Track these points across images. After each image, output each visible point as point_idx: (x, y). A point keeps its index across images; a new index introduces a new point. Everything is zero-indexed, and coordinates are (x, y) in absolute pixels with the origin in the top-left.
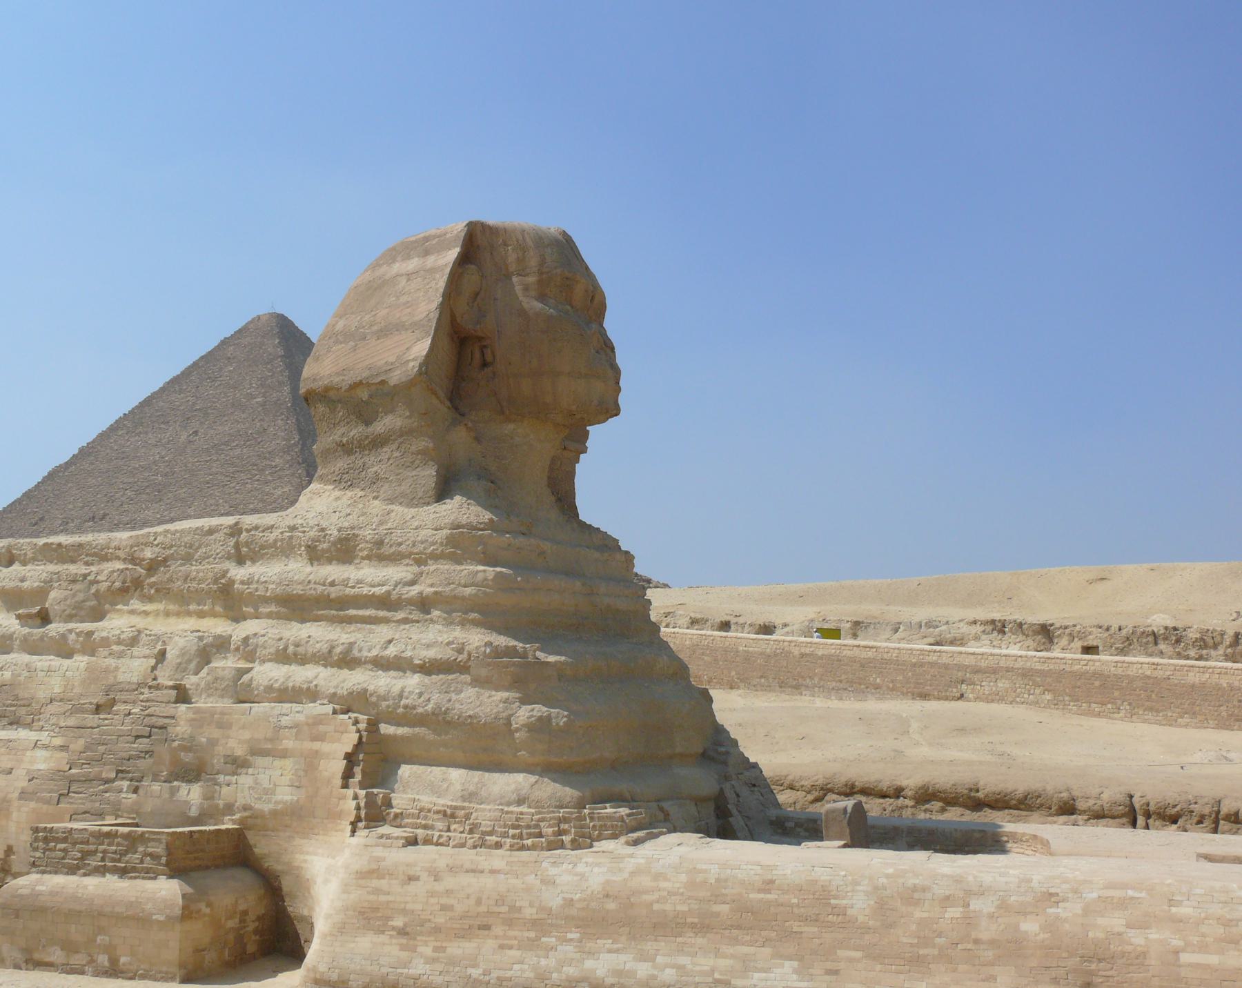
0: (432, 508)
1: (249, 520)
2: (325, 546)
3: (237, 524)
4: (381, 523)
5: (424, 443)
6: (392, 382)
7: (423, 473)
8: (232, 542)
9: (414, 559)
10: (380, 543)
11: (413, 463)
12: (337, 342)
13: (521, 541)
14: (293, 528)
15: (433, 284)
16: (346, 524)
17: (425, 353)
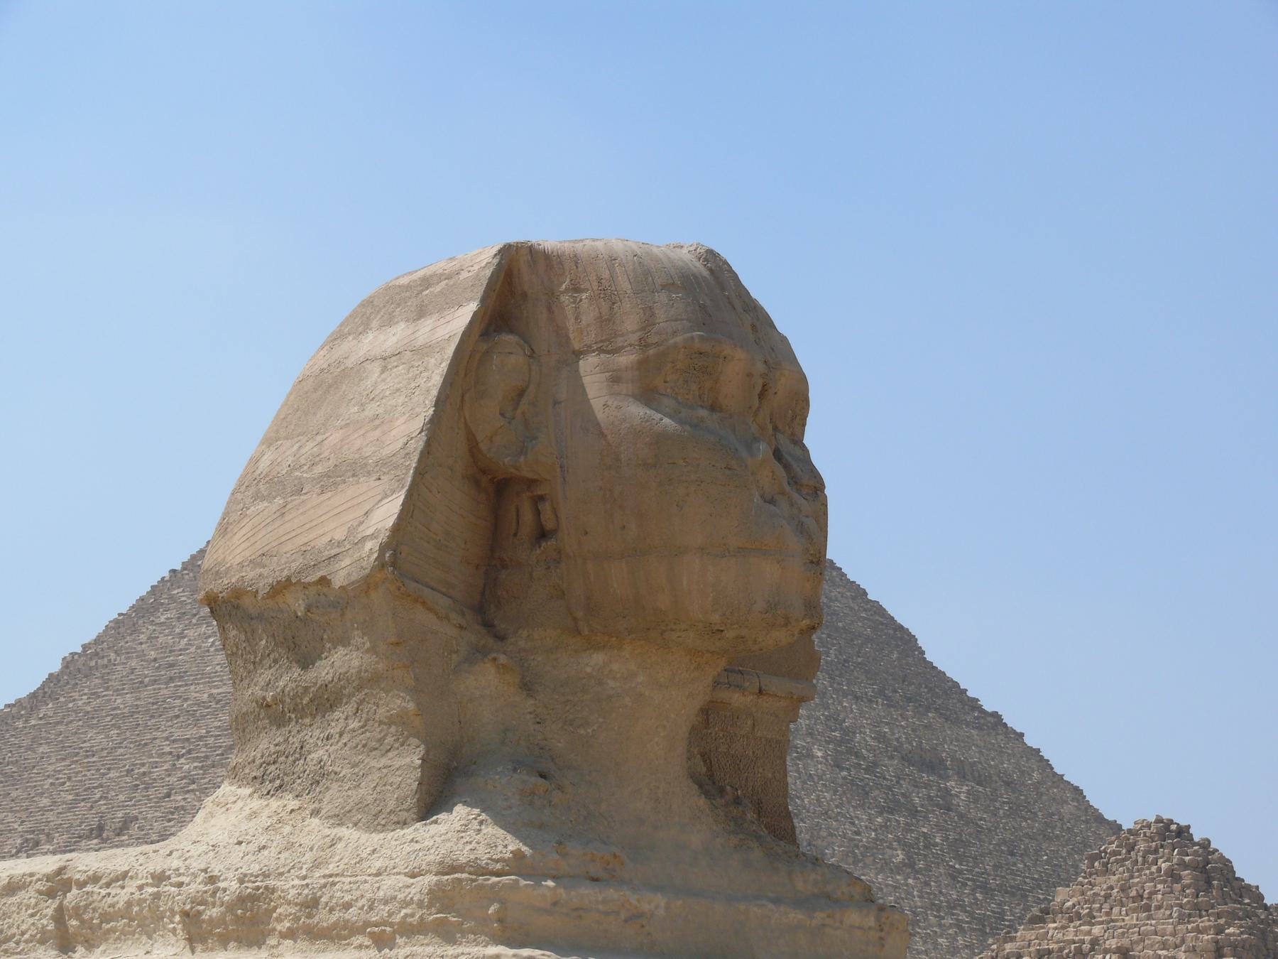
0: (408, 832)
1: (86, 861)
2: (215, 912)
3: (61, 871)
4: (316, 865)
5: (400, 702)
6: (338, 581)
7: (398, 762)
8: (50, 907)
9: (372, 935)
10: (312, 904)
11: (381, 741)
12: (258, 497)
13: (587, 893)
14: (160, 878)
15: (421, 381)
16: (255, 868)
17: (390, 523)
